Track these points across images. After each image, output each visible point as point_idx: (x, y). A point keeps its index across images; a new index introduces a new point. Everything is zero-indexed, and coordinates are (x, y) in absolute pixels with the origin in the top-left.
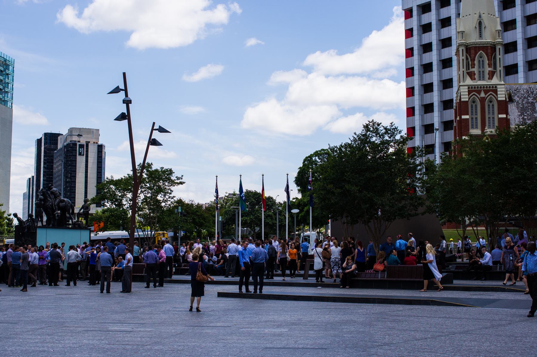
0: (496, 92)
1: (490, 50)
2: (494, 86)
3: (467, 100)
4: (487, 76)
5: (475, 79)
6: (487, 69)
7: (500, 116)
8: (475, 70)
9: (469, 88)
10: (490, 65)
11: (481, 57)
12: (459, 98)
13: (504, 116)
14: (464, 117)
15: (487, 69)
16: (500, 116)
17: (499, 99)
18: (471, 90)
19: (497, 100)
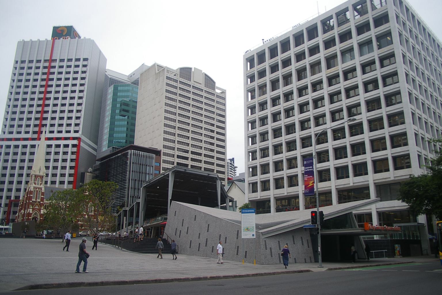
0: (41, 189)
1: (42, 177)
6: (40, 182)
8: (37, 182)
10: (41, 181)
14: (31, 195)
15: (40, 182)
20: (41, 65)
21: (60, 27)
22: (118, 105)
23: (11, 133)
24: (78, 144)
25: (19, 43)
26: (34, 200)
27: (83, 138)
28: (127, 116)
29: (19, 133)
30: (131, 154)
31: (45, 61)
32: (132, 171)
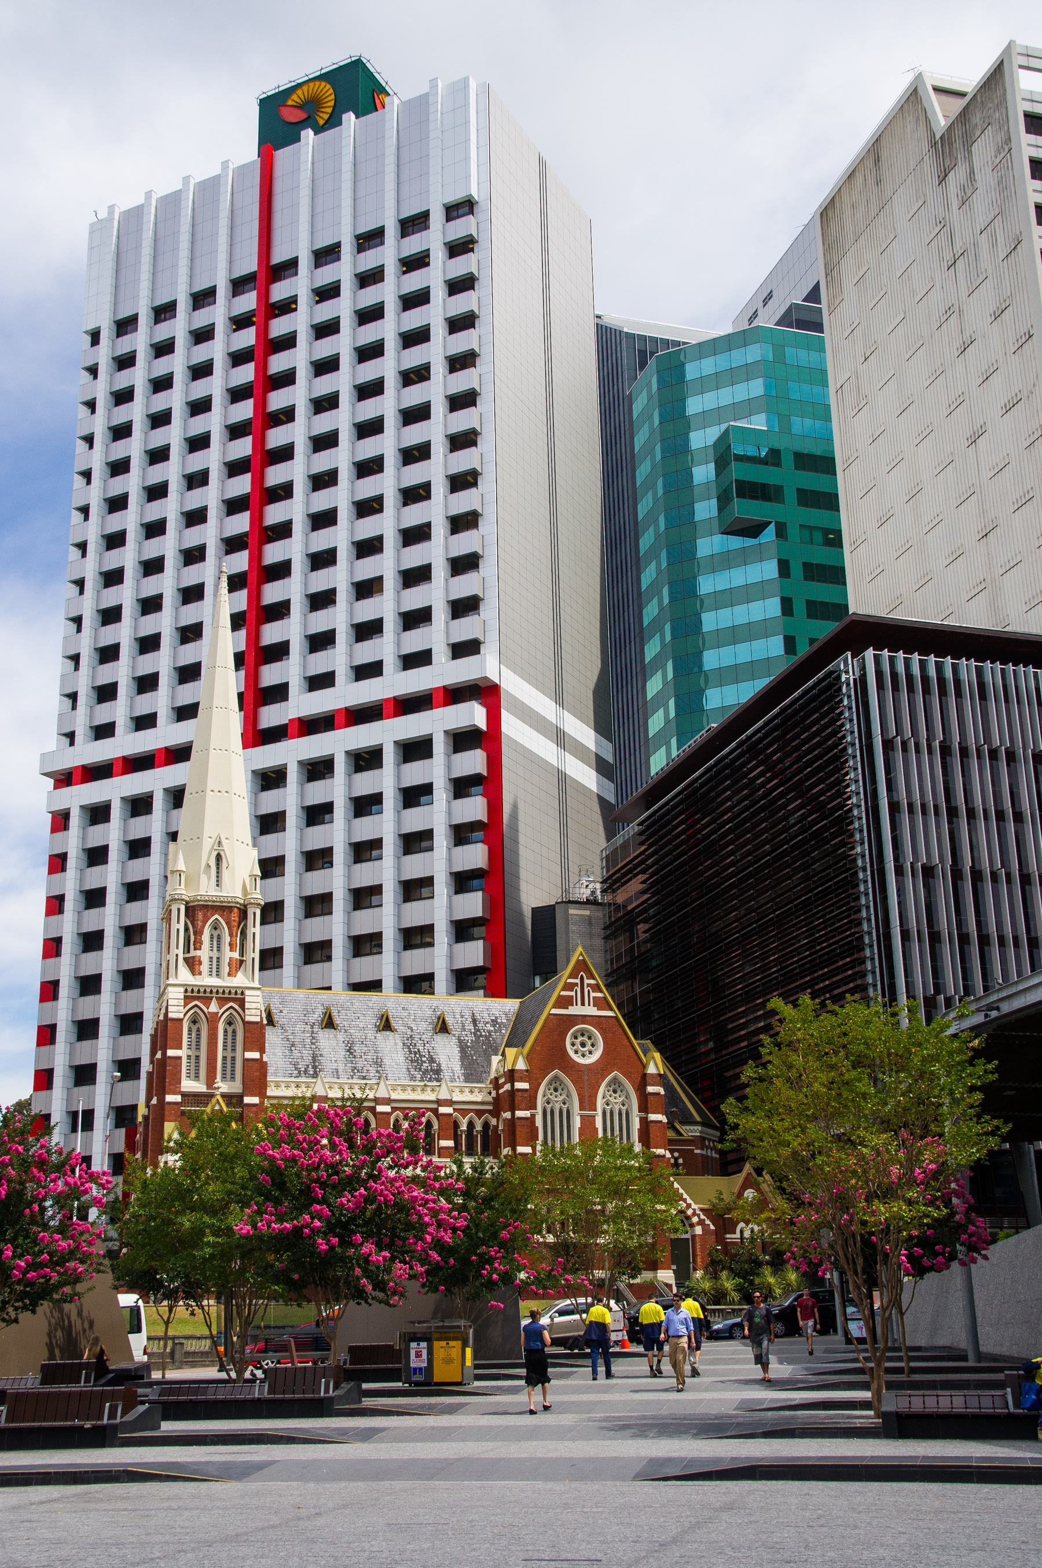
0: (242, 1003)
2: (239, 992)
3: (181, 1016)
4: (226, 969)
5: (200, 973)
6: (230, 955)
7: (249, 1055)
9: (186, 991)
11: (216, 929)
12: (163, 1011)
13: (256, 1055)
14: (171, 1053)
15: (230, 955)
16: (249, 1055)
17: (248, 1019)
18: (191, 995)
19: (243, 1020)
20: (218, 314)
21: (299, 86)
22: (704, 473)
23: (104, 731)
24: (483, 725)
25: (98, 228)
26: (200, 1087)
27: (513, 685)
28: (772, 526)
29: (145, 722)
30: (862, 682)
31: (239, 286)
32: (894, 808)
